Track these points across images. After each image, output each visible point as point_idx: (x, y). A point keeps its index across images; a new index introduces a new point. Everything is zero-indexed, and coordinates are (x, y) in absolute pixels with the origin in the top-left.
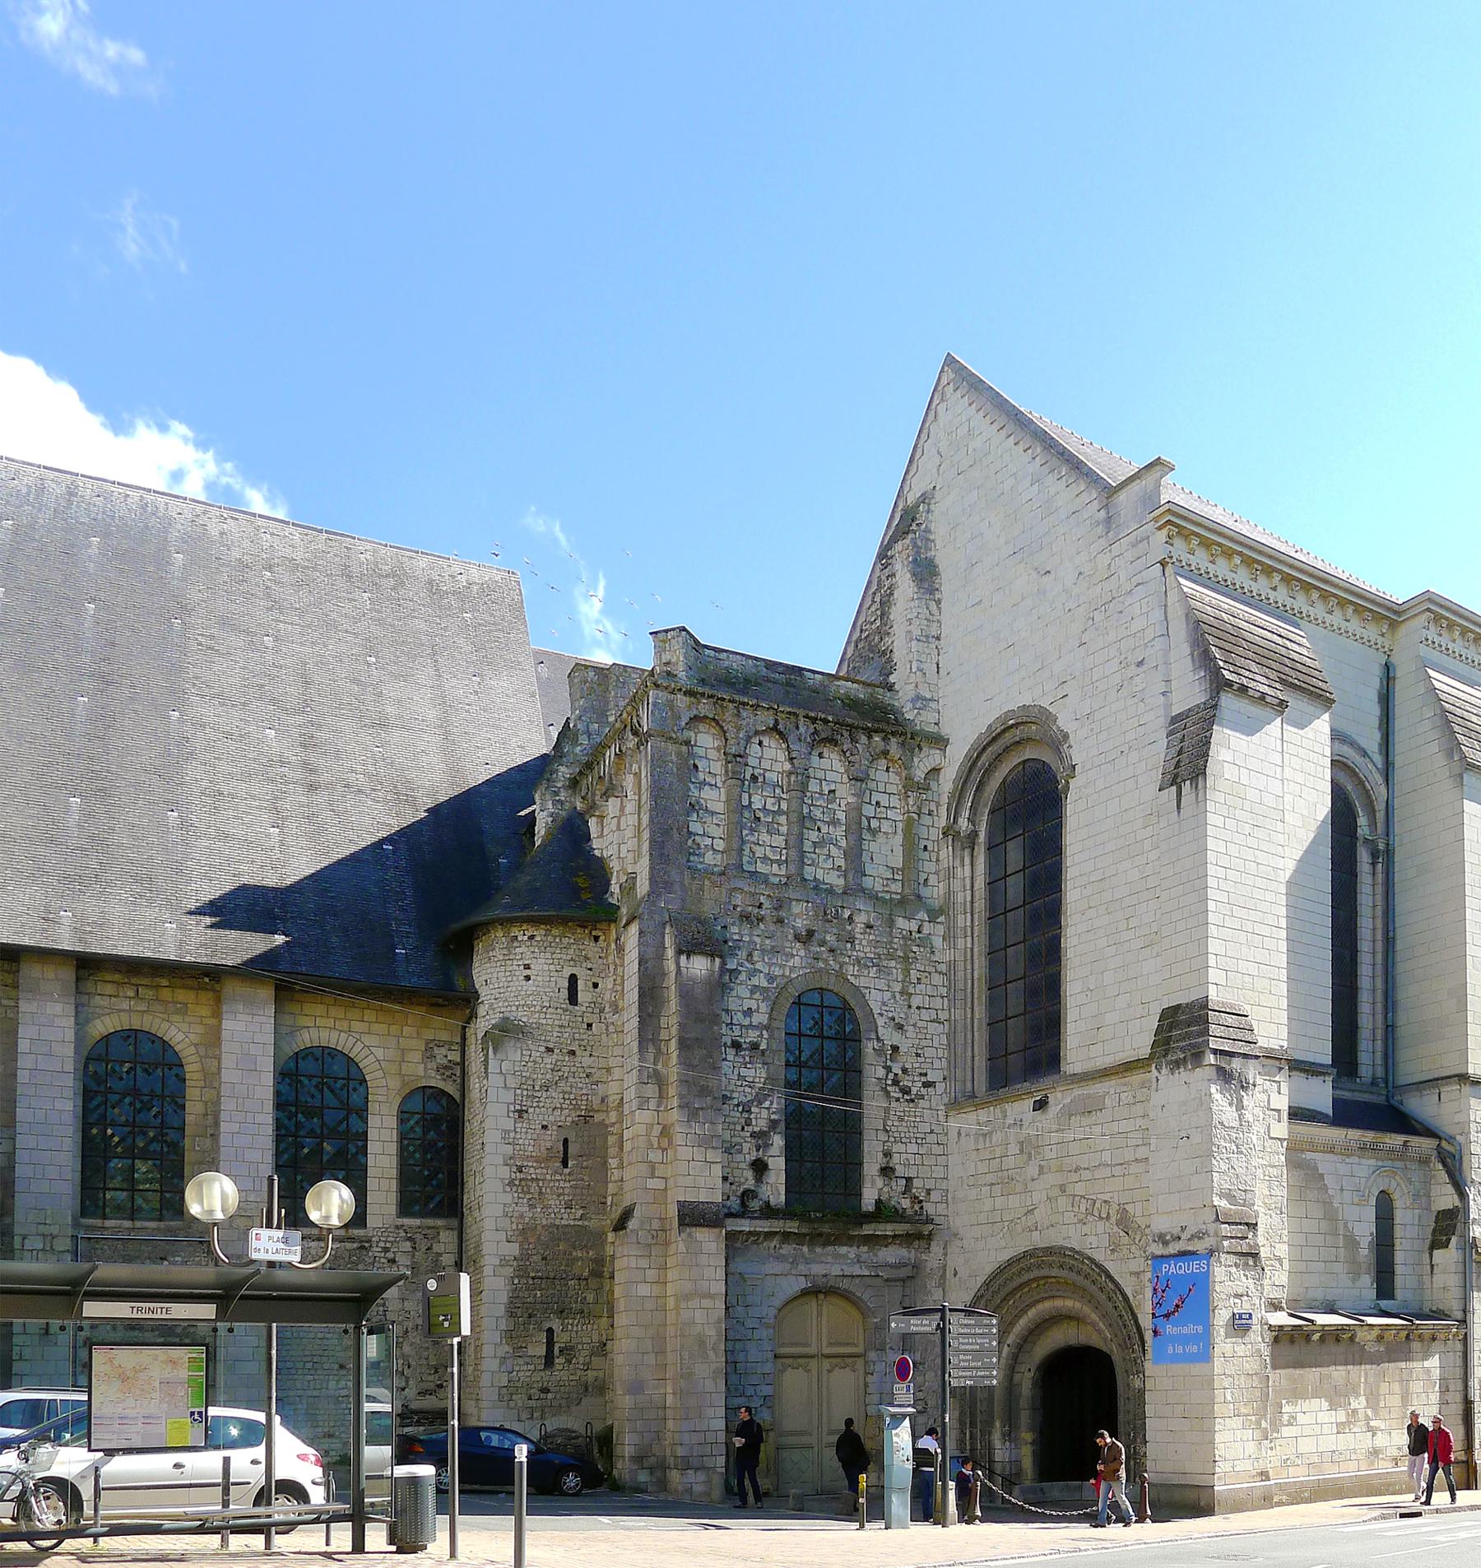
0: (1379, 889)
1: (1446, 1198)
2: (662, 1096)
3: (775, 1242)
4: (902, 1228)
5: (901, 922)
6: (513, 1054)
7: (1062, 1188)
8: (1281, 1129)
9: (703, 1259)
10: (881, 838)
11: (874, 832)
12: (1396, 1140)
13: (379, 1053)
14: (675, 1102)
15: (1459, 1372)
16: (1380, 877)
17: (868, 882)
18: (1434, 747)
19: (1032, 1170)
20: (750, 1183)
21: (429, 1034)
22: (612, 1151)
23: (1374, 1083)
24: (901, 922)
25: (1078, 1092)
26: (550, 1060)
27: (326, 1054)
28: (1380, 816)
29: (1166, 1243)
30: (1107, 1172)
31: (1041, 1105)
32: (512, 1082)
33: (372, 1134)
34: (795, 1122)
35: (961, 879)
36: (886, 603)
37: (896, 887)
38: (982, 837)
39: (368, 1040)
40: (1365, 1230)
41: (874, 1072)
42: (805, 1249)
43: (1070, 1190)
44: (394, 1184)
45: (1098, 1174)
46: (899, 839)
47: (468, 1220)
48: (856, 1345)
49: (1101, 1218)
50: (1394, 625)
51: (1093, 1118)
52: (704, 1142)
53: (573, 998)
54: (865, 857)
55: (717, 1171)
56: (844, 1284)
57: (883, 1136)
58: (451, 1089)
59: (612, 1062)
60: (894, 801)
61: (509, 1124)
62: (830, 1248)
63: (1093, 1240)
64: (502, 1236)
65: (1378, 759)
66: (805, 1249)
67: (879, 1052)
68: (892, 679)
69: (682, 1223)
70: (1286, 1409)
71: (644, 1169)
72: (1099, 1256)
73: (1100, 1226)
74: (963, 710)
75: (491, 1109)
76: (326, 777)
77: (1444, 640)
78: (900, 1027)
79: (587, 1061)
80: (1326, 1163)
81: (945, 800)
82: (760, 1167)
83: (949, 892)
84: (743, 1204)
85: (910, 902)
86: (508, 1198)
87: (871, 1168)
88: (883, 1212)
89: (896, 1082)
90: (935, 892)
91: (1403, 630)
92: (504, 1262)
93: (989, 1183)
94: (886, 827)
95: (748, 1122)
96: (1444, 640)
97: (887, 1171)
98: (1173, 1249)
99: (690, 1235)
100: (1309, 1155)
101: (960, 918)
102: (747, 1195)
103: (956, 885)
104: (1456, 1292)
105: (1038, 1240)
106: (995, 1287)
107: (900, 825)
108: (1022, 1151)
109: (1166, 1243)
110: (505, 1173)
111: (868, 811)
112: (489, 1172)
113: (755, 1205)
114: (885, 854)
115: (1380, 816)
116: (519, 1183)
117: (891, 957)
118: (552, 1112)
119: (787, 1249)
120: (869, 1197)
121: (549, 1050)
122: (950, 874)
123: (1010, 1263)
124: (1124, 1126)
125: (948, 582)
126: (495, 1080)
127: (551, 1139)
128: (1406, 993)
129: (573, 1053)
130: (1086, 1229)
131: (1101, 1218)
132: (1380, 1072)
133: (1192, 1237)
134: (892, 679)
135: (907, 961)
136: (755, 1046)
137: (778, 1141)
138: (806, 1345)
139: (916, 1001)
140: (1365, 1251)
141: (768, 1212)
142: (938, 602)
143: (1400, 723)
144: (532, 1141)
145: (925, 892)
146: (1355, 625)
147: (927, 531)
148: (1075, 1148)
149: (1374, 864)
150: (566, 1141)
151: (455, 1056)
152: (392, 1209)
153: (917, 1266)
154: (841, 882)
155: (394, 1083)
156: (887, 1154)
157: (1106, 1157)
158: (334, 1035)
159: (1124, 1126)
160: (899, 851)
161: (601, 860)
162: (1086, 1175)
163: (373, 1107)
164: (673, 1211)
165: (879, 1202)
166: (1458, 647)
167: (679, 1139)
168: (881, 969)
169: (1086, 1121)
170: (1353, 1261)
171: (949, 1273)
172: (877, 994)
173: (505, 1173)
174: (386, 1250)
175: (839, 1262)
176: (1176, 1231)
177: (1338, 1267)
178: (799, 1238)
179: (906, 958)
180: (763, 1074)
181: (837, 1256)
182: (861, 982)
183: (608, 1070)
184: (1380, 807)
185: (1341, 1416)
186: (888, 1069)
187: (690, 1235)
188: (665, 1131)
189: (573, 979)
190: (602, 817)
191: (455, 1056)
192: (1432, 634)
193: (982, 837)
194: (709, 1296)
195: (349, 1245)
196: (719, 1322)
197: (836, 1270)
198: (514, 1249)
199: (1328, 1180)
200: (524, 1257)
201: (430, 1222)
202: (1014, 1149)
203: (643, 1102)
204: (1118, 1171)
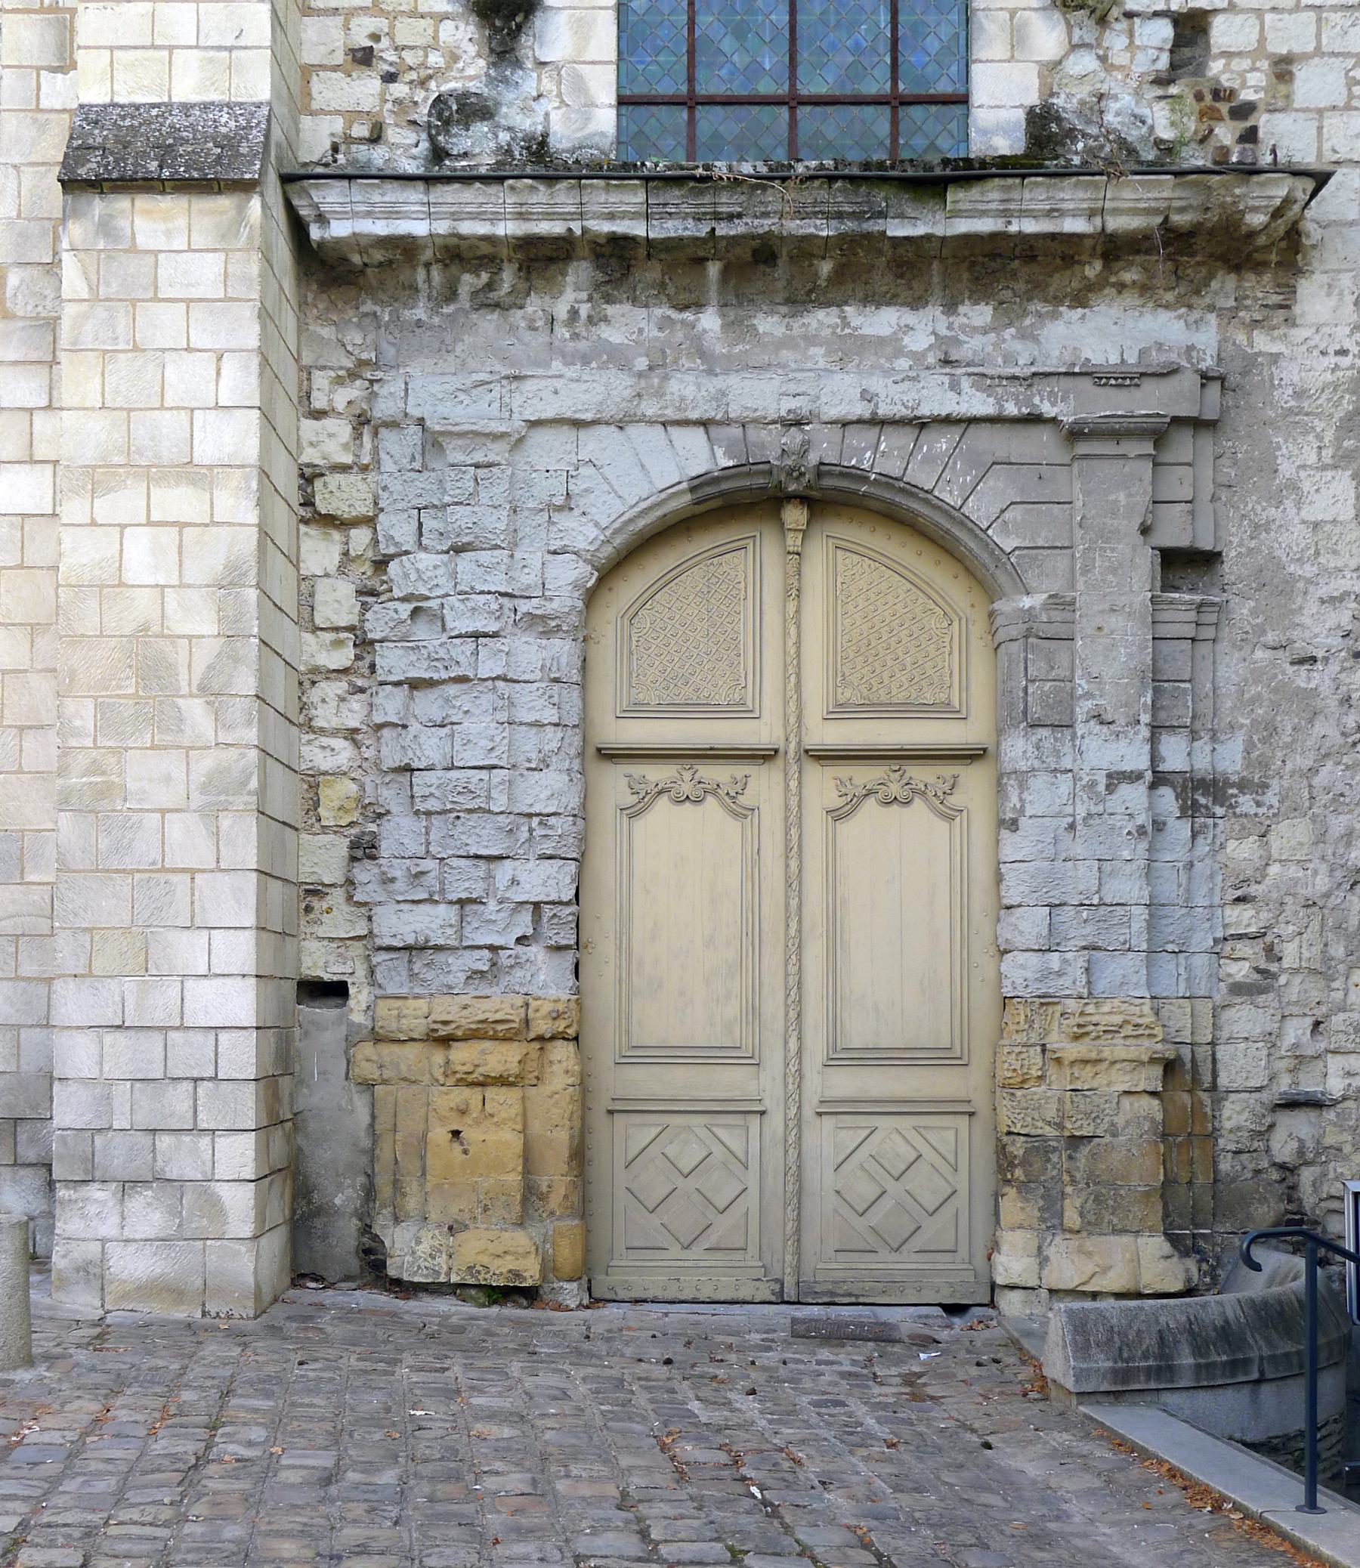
9: (163, 325)
20: (471, 72)
42: (710, 321)
48: (945, 711)
56: (882, 457)
62: (822, 319)
66: (710, 321)
99: (106, 228)
119: (630, 324)
138: (740, 711)
141: (540, 162)
181: (849, 350)
187: (106, 228)
194: (191, 472)
196: (227, 583)
197: (841, 394)
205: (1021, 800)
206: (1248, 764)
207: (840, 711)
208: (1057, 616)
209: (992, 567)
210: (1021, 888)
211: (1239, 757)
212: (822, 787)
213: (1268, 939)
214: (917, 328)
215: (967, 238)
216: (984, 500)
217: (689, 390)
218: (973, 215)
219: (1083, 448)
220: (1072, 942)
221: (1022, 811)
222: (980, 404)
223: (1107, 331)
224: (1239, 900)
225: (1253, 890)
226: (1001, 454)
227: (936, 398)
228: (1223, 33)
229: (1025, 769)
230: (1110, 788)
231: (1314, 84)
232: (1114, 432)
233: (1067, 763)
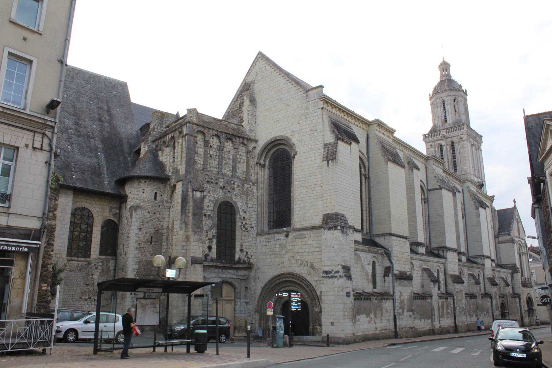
0: (367, 186)
1: (387, 264)
2: (186, 228)
3: (213, 268)
4: (245, 266)
5: (246, 185)
6: (139, 212)
7: (293, 257)
8: (353, 245)
10: (241, 163)
11: (239, 162)
12: (375, 249)
13: (97, 210)
14: (191, 229)
15: (392, 308)
16: (367, 183)
17: (237, 174)
18: (380, 154)
19: (284, 252)
20: (207, 252)
21: (111, 205)
22: (164, 240)
23: (367, 233)
24: (246, 185)
25: (298, 233)
26: (149, 215)
27: (84, 209)
28: (367, 169)
29: (327, 274)
30: (307, 254)
31: (287, 236)
32: (139, 220)
33: (94, 232)
34: (220, 237)
35: (263, 175)
36: (241, 105)
37: (244, 176)
38: (267, 165)
39: (94, 206)
40: (370, 271)
41: (239, 224)
43: (295, 258)
44: (99, 246)
45: (304, 254)
46: (245, 164)
47: (120, 258)
50: (369, 125)
51: (302, 240)
52: (198, 241)
53: (155, 199)
54: (237, 168)
55: (201, 248)
56: (230, 280)
57: (241, 241)
58: (116, 220)
59: (165, 216)
60: (244, 154)
61: (137, 232)
63: (303, 272)
64: (134, 263)
65: (366, 156)
67: (240, 218)
68: (243, 124)
69: (192, 263)
70: (357, 317)
71: (181, 247)
73: (305, 268)
74: (264, 135)
75: (133, 227)
76: (82, 133)
77: (380, 130)
78: (245, 212)
79: (158, 216)
80: (361, 254)
81: (257, 155)
82: (210, 248)
83: (257, 179)
84: (206, 257)
85: (247, 180)
86: (136, 252)
87: (238, 249)
88: (239, 261)
89: (244, 227)
90: (253, 178)
91: (371, 126)
92: (134, 270)
93: (268, 255)
94: (242, 161)
95: (207, 236)
96: (380, 130)
97: (241, 250)
98: (329, 275)
100: (358, 252)
101: (261, 185)
102: (206, 256)
103: (259, 177)
104: (391, 287)
105: (285, 270)
106: (272, 282)
107: (245, 161)
108: (280, 247)
109: (327, 274)
110: (136, 245)
111: (238, 156)
112: (131, 245)
113: (209, 258)
114: (241, 168)
115: (367, 169)
116: (139, 248)
117: (243, 194)
118: (149, 229)
119: (216, 270)
120: (237, 257)
121: (149, 212)
122: (258, 174)
123: (277, 276)
124: (312, 242)
125: (258, 101)
126: (134, 220)
127: (148, 236)
128: (375, 212)
129: (155, 213)
130: (300, 268)
132: (368, 231)
133: (336, 272)
134: (243, 124)
135: (247, 195)
136: (209, 215)
137: (215, 241)
139: (249, 205)
140: (370, 277)
141: (212, 260)
142: (256, 107)
143: (371, 148)
144: (143, 237)
145: (251, 177)
146: (361, 125)
147: (253, 90)
148: (297, 247)
149: (365, 180)
150: (152, 237)
151: (117, 212)
152: (98, 253)
153: (249, 276)
154: (231, 174)
155: (101, 218)
156: (242, 246)
157: (307, 250)
158: (86, 204)
159: (312, 242)
160: (245, 167)
161: (162, 162)
162: (300, 254)
163: (95, 224)
164: (189, 259)
165: (239, 258)
166: (383, 131)
167: (192, 240)
168: (241, 198)
169: (300, 240)
170: (368, 279)
171: (256, 278)
172: (240, 204)
173: (136, 245)
174: (95, 265)
175: (229, 275)
176: (330, 270)
177: (365, 281)
178: (219, 267)
179: (247, 195)
180: (211, 222)
182: (236, 200)
183: (164, 218)
184: (367, 167)
185: (368, 319)
186: (242, 223)
188: (187, 238)
189: (156, 194)
190: (163, 151)
191: (117, 212)
192: (378, 128)
193: (267, 165)
195: (85, 263)
197: (228, 276)
198: (136, 267)
199: (362, 259)
200: (139, 268)
201: (108, 257)
202: (278, 246)
203: (181, 229)
204: (310, 254)
207: (226, 297)
212: (224, 302)
214: (232, 271)
215: (107, 161)
216: (236, 284)
217: (220, 275)
218: (237, 266)
222: (236, 277)
223: (242, 273)
227: (234, 277)
228: (249, 253)
231: (253, 257)
232: (243, 279)
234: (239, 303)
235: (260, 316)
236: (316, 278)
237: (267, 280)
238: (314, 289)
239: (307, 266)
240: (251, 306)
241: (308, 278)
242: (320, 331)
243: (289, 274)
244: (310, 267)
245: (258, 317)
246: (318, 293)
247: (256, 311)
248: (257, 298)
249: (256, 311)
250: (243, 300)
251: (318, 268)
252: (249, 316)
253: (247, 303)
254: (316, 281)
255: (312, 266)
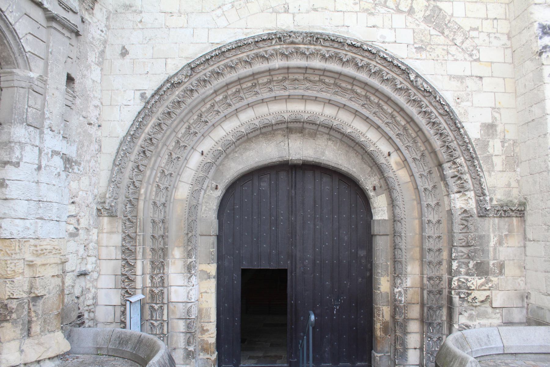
49: (399, 11)
72: (401, 53)
73: (399, 20)
130: (372, 21)
131: (401, 12)
205: (21, 154)
206: (77, 156)
208: (40, 84)
209: (17, 55)
210: (18, 192)
211: (75, 152)
213: (78, 217)
219: (54, 25)
220: (32, 216)
221: (21, 159)
224: (73, 203)
225: (75, 199)
226: (28, 12)
229: (23, 142)
230: (52, 155)
233: (37, 143)
234: (30, 155)
235: (129, 237)
236: (461, 67)
237: (175, 65)
238: (449, 114)
239: (411, 11)
240: (85, 181)
241: (423, 67)
242: (481, 295)
243: (315, 38)
244: (427, 19)
245: (117, 239)
246: (473, 130)
247: (104, 210)
248: (111, 147)
249: (104, 210)
250: (53, 142)
251: (466, 25)
252: (73, 235)
253: (68, 162)
254: (461, 79)
255: (436, 18)
